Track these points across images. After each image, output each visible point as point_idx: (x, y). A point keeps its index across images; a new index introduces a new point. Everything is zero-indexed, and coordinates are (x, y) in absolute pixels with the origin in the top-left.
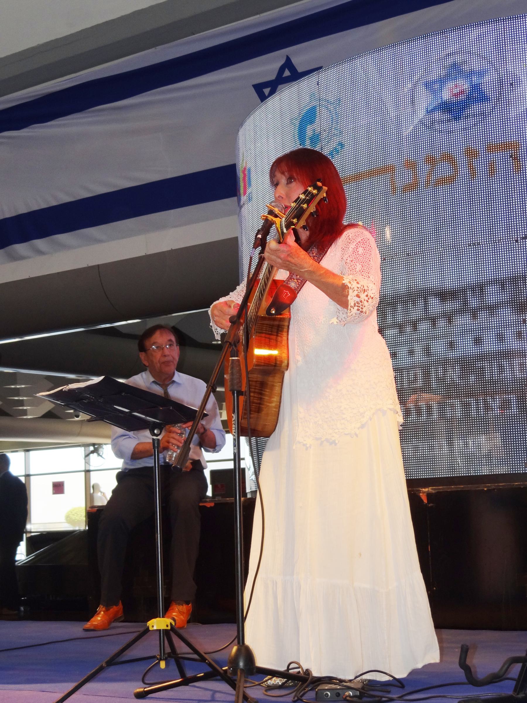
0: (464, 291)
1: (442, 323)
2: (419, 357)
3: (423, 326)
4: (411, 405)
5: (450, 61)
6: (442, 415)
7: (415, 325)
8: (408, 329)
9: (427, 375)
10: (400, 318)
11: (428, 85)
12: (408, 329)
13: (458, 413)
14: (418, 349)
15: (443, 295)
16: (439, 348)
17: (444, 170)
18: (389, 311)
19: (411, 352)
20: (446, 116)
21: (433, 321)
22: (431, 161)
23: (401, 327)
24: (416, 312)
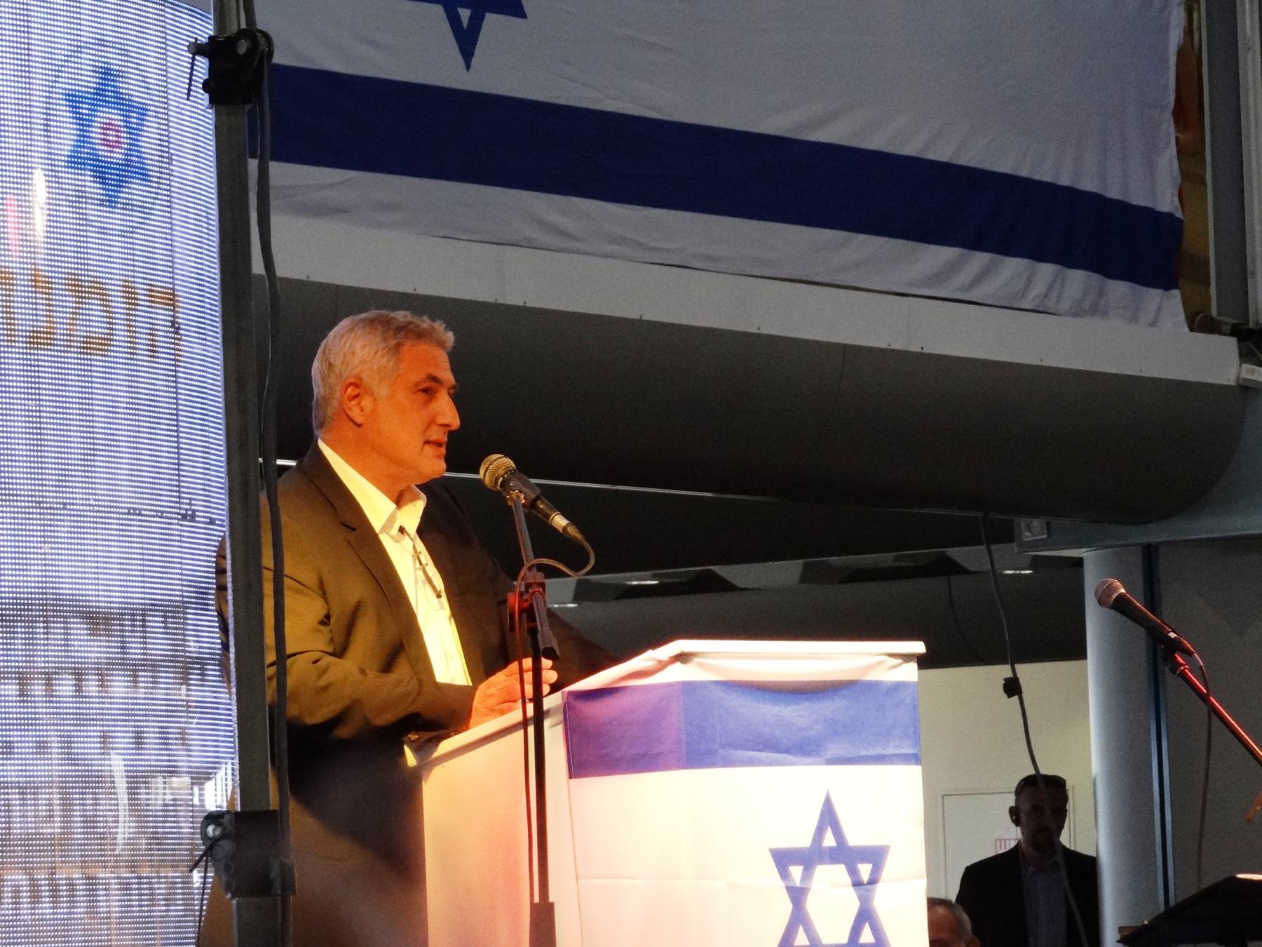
1: (92, 687)
3: (65, 687)
4: (41, 875)
6: (92, 910)
7: (49, 681)
8: (38, 689)
9: (66, 804)
11: (73, 100)
12: (38, 689)
13: (115, 907)
14: (54, 742)
15: (98, 621)
16: (88, 744)
19: (42, 747)
21: (79, 676)
23: (23, 680)
24: (47, 654)
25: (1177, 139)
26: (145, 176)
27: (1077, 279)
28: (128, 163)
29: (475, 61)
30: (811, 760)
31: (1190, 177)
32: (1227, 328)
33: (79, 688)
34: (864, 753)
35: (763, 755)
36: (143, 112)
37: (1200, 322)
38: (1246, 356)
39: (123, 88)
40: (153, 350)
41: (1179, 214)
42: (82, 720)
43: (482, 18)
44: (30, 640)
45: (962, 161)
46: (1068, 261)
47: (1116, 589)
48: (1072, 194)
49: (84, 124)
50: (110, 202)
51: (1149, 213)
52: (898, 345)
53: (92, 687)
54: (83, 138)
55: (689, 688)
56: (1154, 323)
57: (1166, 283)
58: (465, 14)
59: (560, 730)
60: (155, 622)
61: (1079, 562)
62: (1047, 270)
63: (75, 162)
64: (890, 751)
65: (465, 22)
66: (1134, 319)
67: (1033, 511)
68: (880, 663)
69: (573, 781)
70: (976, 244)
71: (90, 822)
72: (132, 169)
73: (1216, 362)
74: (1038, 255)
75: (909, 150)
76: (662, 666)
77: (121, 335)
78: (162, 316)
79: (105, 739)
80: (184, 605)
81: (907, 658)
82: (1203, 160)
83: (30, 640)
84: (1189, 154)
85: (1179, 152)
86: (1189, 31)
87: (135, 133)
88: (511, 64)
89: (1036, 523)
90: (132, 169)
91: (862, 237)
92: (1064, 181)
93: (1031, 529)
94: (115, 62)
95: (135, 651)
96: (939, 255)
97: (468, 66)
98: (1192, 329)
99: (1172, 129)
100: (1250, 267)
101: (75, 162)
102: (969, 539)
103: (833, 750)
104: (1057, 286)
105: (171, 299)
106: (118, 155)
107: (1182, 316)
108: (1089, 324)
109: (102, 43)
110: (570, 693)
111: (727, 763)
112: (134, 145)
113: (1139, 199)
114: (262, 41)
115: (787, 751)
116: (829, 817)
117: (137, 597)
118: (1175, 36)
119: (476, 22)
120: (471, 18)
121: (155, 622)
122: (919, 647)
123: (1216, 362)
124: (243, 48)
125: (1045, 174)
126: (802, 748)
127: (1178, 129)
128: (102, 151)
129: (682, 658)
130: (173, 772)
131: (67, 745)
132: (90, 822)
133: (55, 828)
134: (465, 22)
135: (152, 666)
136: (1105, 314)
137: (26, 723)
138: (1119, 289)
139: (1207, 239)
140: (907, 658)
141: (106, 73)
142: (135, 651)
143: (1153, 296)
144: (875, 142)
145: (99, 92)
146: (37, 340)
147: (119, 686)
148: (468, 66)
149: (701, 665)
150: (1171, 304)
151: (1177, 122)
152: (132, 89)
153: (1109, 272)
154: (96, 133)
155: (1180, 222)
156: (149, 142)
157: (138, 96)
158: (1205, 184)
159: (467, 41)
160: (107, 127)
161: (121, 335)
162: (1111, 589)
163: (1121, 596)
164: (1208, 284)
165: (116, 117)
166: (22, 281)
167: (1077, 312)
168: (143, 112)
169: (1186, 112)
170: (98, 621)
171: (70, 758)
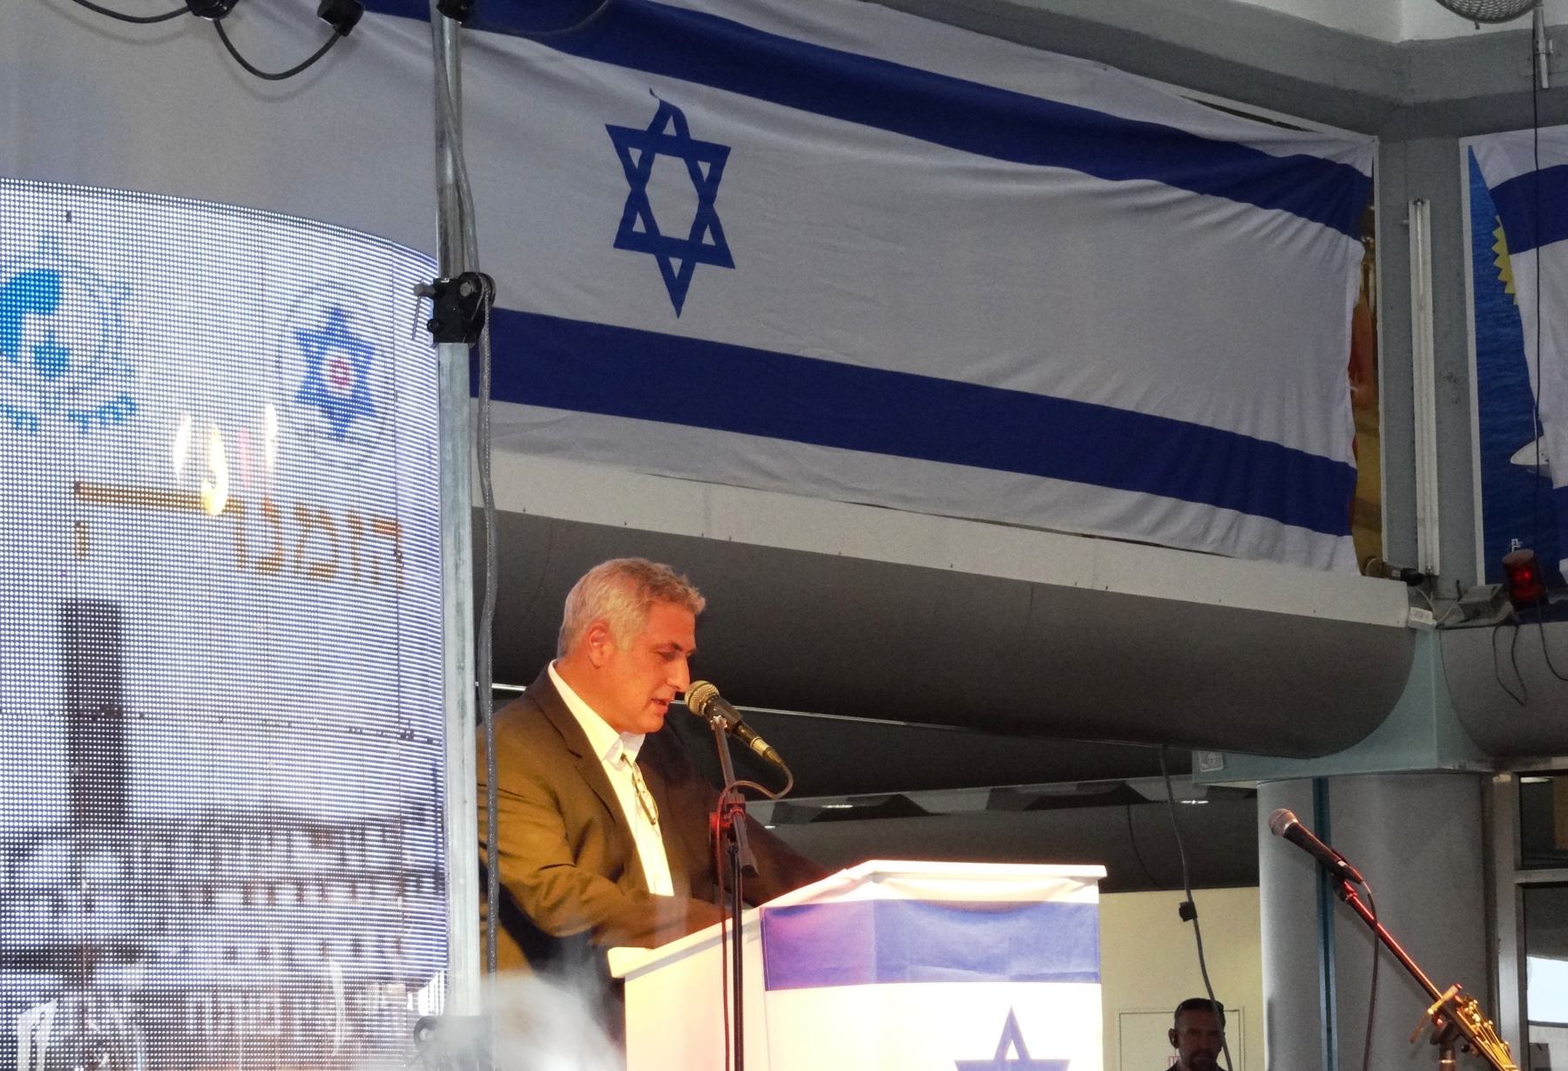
0: (340, 830)
2: (277, 970)
3: (286, 896)
5: (332, 298)
7: (271, 890)
8: (260, 897)
9: (287, 1007)
10: (244, 870)
11: (303, 338)
12: (260, 897)
14: (276, 947)
15: (319, 834)
16: (307, 950)
17: (319, 548)
18: (225, 845)
19: (264, 953)
20: (325, 424)
21: (300, 885)
22: (302, 514)
23: (247, 889)
24: (273, 862)
25: (1352, 393)
26: (369, 410)
27: (1255, 524)
28: (355, 399)
29: (684, 308)
30: (994, 976)
31: (1365, 428)
32: (1396, 573)
33: (300, 897)
34: (1046, 971)
35: (951, 971)
36: (369, 351)
37: (1372, 566)
38: (1414, 601)
39: (353, 327)
40: (376, 577)
41: (1353, 464)
42: (302, 928)
43: (692, 268)
44: (255, 852)
45: (1146, 411)
46: (1245, 506)
47: (1289, 819)
48: (1251, 442)
49: (314, 361)
50: (339, 436)
51: (1324, 461)
52: (1084, 584)
53: (312, 895)
54: (314, 373)
55: (881, 906)
56: (1329, 567)
57: (1340, 531)
58: (676, 264)
59: (757, 944)
60: (373, 835)
61: (1252, 794)
62: (1226, 515)
63: (304, 397)
64: (1072, 969)
65: (676, 271)
66: (1309, 562)
67: (1210, 745)
68: (1063, 886)
69: (770, 993)
70: (1159, 488)
71: (308, 1025)
72: (360, 404)
73: (1389, 605)
74: (1218, 502)
75: (1097, 398)
76: (855, 884)
77: (346, 562)
78: (385, 546)
79: (324, 946)
80: (402, 820)
81: (1088, 881)
82: (1377, 414)
83: (255, 852)
84: (1364, 406)
85: (1354, 405)
86: (1365, 291)
87: (362, 370)
88: (718, 312)
89: (1212, 755)
90: (360, 404)
91: (1051, 482)
92: (1244, 430)
93: (1208, 764)
94: (347, 304)
95: (354, 863)
96: (1124, 500)
97: (679, 312)
98: (1363, 574)
99: (1348, 383)
100: (1420, 515)
101: (304, 397)
102: (1151, 771)
103: (1017, 967)
104: (1234, 533)
105: (394, 529)
106: (347, 392)
107: (1354, 561)
108: (1265, 567)
109: (332, 284)
110: (768, 909)
111: (915, 978)
112: (362, 382)
113: (1315, 449)
114: (484, 285)
115: (974, 968)
116: (1012, 1031)
117: (355, 812)
118: (1351, 298)
119: (687, 271)
120: (683, 267)
121: (373, 835)
122: (1100, 871)
123: (1389, 605)
124: (467, 289)
125: (1225, 425)
126: (987, 965)
127: (1353, 384)
128: (331, 387)
129: (876, 877)
130: (387, 979)
131: (289, 951)
132: (308, 1025)
133: (276, 1031)
134: (676, 271)
135: (371, 878)
136: (1280, 560)
137: (247, 931)
138: (1295, 534)
139: (1380, 487)
140: (1088, 881)
141: (337, 314)
142: (354, 863)
143: (1327, 541)
144: (1062, 392)
145: (329, 331)
146: (270, 565)
147: (339, 895)
148: (679, 312)
149: (892, 884)
150: (1345, 549)
151: (1352, 377)
152: (358, 327)
153: (1285, 520)
154: (326, 370)
155: (1354, 471)
156: (374, 380)
157: (367, 336)
158: (1377, 435)
159: (678, 289)
160: (337, 364)
161: (346, 562)
162: (1284, 818)
163: (1294, 827)
164: (1379, 530)
165: (346, 357)
166: (254, 509)
167: (1255, 554)
168: (369, 351)
169: (1362, 366)
170: (319, 834)
171: (291, 964)
